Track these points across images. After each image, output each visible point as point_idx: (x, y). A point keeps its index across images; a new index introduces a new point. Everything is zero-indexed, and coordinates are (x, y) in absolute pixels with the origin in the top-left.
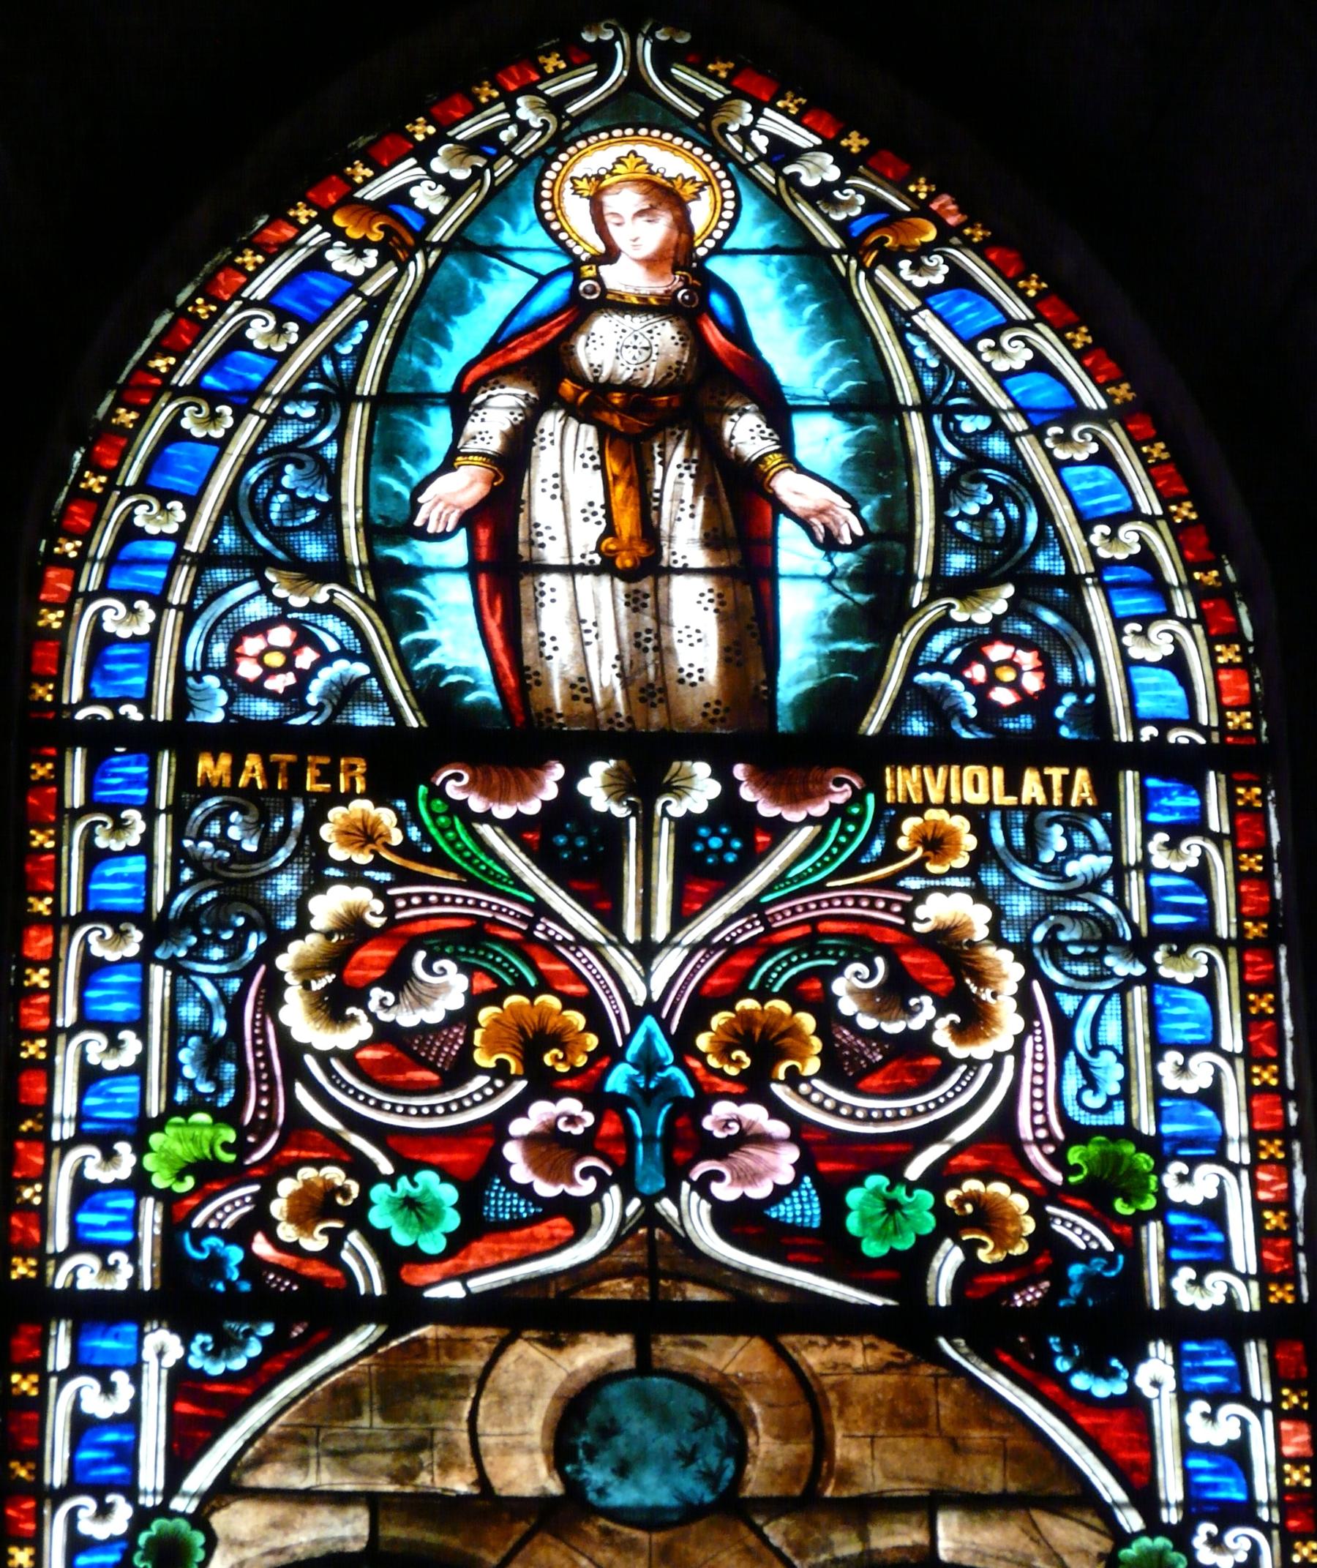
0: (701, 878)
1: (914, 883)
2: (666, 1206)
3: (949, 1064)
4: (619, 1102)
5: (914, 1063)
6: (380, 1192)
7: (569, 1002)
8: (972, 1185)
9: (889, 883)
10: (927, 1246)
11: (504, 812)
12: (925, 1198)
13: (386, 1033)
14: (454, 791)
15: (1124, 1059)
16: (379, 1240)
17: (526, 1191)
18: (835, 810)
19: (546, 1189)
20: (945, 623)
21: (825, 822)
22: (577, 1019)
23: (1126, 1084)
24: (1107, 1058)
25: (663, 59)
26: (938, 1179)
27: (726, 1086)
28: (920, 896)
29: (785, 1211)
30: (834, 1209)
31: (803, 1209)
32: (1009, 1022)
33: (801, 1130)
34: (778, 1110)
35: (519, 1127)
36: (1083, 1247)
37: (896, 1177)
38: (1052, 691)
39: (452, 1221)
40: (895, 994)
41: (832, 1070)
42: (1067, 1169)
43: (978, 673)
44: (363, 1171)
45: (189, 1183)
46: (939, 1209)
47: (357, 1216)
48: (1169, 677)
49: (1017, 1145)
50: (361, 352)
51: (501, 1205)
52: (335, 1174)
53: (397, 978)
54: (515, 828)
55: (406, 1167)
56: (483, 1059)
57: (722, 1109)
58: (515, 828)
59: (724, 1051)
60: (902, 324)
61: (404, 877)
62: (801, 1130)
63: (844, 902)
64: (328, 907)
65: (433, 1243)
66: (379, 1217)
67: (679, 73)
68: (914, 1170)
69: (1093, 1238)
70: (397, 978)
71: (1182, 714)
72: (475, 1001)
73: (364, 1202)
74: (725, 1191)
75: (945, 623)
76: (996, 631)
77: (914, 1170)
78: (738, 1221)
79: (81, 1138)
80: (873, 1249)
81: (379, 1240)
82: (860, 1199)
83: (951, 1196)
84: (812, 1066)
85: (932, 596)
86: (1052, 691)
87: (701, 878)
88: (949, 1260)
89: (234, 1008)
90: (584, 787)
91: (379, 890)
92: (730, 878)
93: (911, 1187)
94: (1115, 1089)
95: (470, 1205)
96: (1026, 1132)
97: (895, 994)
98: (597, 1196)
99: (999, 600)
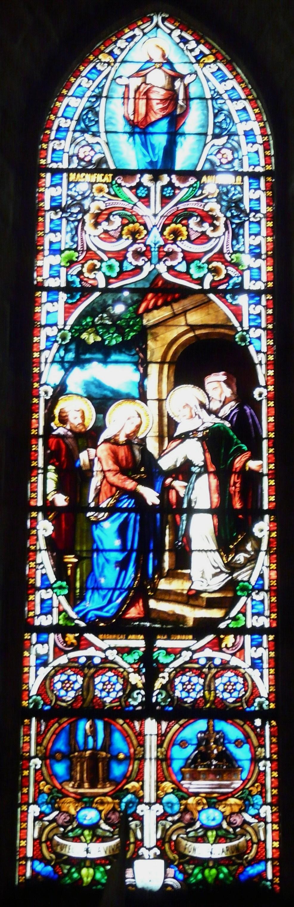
0: (165, 200)
1: (206, 201)
2: (158, 266)
4: (149, 245)
5: (204, 238)
7: (141, 224)
9: (201, 201)
10: (205, 275)
11: (128, 185)
12: (206, 265)
13: (106, 232)
14: (119, 181)
18: (191, 186)
20: (213, 145)
21: (189, 187)
22: (142, 228)
25: (164, 20)
27: (169, 242)
28: (206, 203)
29: (178, 268)
30: (188, 268)
31: (182, 268)
32: (222, 229)
33: (183, 251)
34: (178, 246)
38: (234, 159)
40: (200, 223)
41: (189, 239)
43: (219, 156)
44: (101, 261)
45: (68, 264)
48: (256, 155)
49: (224, 254)
50: (103, 86)
51: (127, 266)
52: (95, 262)
53: (108, 220)
54: (131, 188)
55: (110, 258)
57: (168, 246)
58: (131, 188)
59: (169, 234)
60: (208, 81)
61: (109, 200)
62: (183, 251)
63: (192, 204)
64: (94, 209)
65: (114, 275)
66: (104, 269)
67: (166, 23)
68: (204, 259)
70: (108, 220)
71: (257, 163)
72: (123, 225)
74: (169, 263)
75: (213, 145)
76: (224, 146)
77: (204, 259)
78: (171, 269)
80: (195, 276)
82: (193, 266)
84: (185, 238)
85: (213, 139)
86: (234, 159)
87: (165, 200)
89: (76, 228)
90: (143, 180)
91: (104, 202)
92: (171, 198)
95: (121, 266)
96: (225, 251)
97: (200, 223)
99: (224, 140)
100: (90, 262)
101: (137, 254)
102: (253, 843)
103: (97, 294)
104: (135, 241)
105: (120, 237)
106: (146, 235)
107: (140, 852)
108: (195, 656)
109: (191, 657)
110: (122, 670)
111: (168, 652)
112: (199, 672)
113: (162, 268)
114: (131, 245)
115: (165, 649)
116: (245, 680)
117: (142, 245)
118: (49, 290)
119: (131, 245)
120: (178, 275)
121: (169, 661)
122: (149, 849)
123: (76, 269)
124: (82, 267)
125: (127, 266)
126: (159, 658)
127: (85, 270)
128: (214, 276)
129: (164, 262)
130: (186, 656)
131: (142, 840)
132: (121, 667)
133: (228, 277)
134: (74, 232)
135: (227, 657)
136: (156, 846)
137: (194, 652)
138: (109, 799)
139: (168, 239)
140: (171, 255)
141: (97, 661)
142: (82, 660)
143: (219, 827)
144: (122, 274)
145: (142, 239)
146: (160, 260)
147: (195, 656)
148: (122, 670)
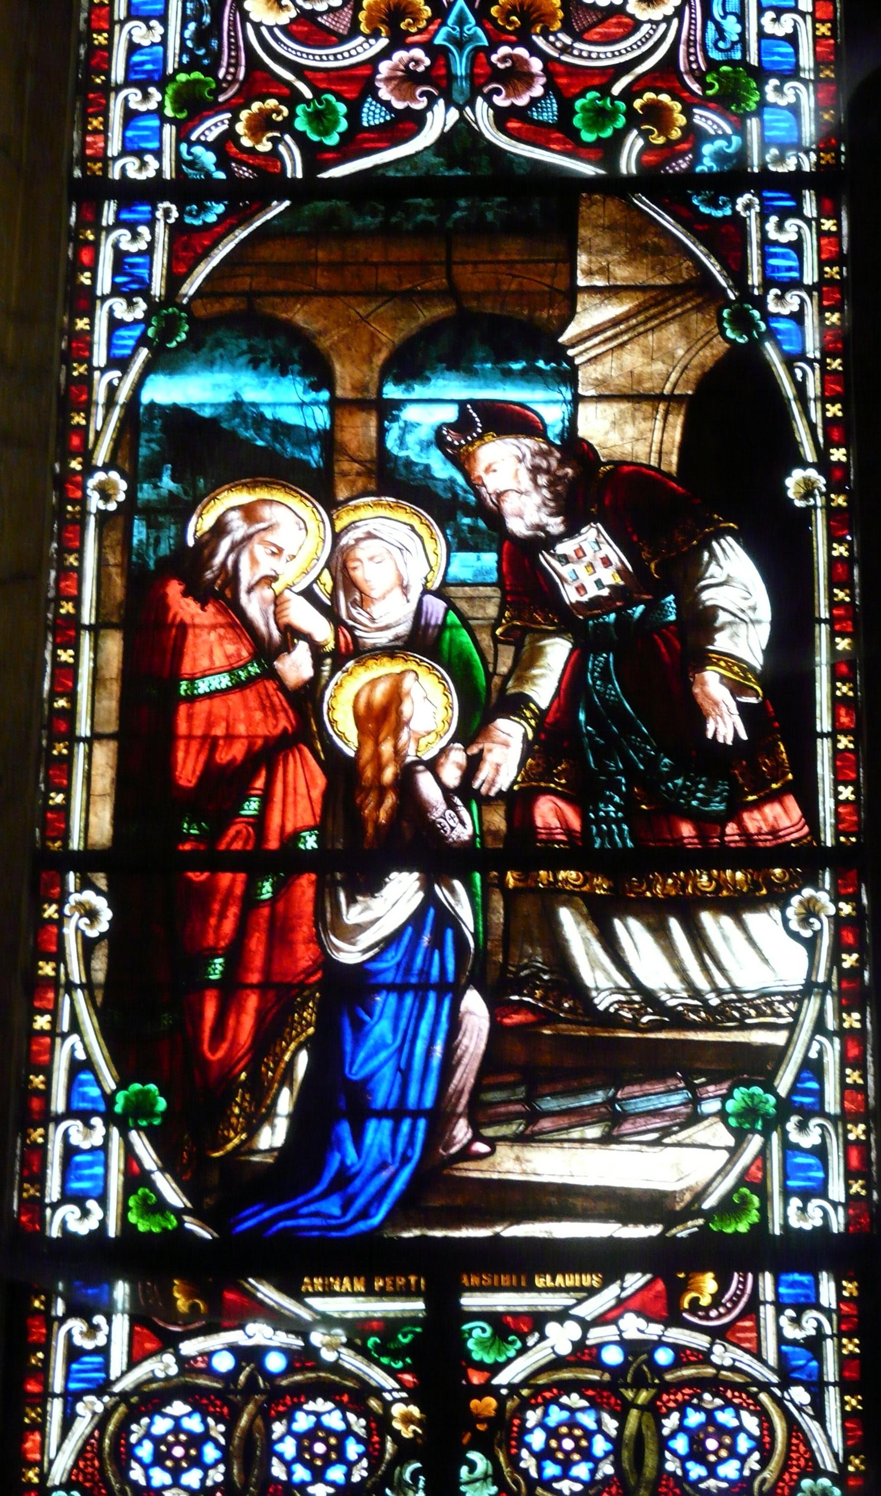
3: (637, 24)
6: (300, 109)
8: (649, 96)
10: (620, 136)
12: (622, 106)
15: (741, 19)
16: (300, 138)
17: (387, 104)
19: (399, 105)
23: (742, 35)
24: (732, 19)
26: (629, 95)
30: (566, 111)
35: (384, 68)
36: (712, 132)
37: (605, 91)
39: (343, 125)
42: (705, 86)
44: (292, 98)
46: (630, 113)
47: (287, 126)
51: (372, 115)
56: (363, 28)
65: (333, 140)
66: (300, 124)
68: (616, 90)
69: (719, 126)
73: (293, 115)
79: (128, 83)
81: (300, 138)
83: (637, 104)
88: (633, 143)
93: (614, 99)
94: (736, 38)
95: (354, 116)
98: (429, 107)
100: (256, 106)
101: (408, 79)
103: (278, 208)
104: (399, 41)
105: (354, 31)
106: (430, 21)
109: (579, 1346)
111: (504, 1327)
112: (607, 1395)
113: (482, 116)
114: (385, 54)
115: (492, 1318)
116: (763, 1415)
117: (418, 53)
118: (131, 194)
119: (385, 54)
120: (537, 134)
121: (502, 1359)
123: (212, 128)
124: (234, 120)
125: (372, 115)
127: (240, 128)
128: (645, 134)
129: (488, 98)
130: (561, 1338)
133: (695, 135)
134: (207, 19)
135: (701, 1341)
137: (586, 1325)
139: (503, 30)
140: (517, 77)
144: (356, 142)
145: (420, 32)
146: (475, 91)
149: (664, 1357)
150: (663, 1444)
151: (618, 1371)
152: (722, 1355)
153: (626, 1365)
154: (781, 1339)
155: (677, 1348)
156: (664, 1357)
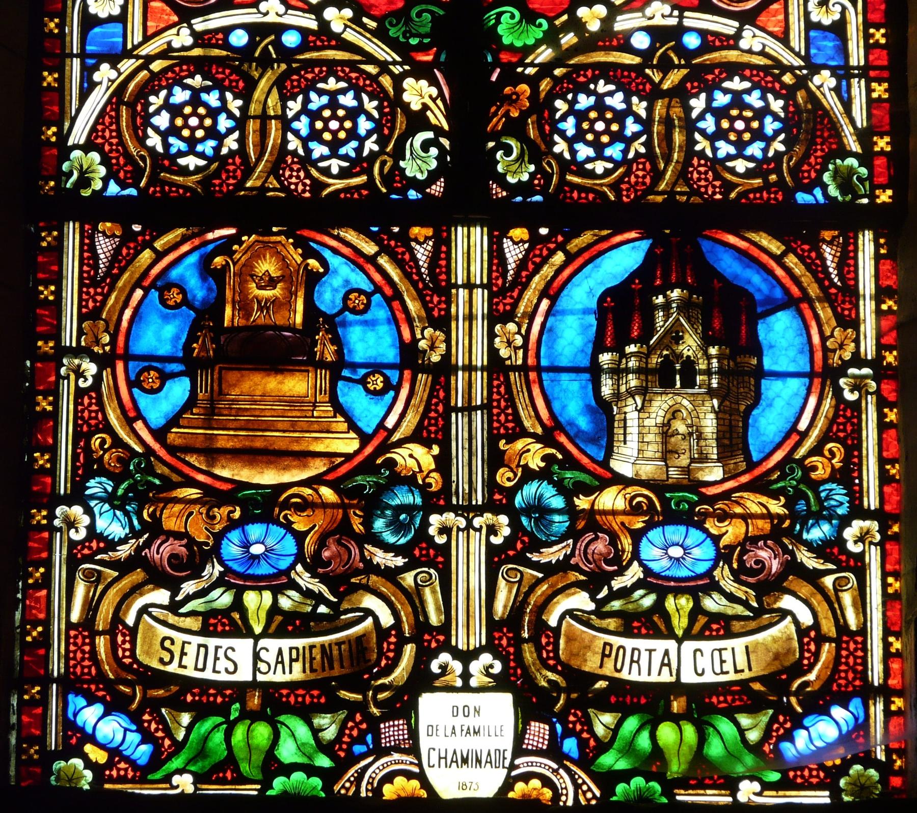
102: (821, 639)
107: (435, 667)
108: (622, 23)
110: (371, 69)
121: (530, 42)
122: (465, 657)
126: (501, 30)
131: (446, 628)
132: (370, 59)
135: (727, 26)
136: (490, 646)
138: (327, 493)
141: (291, 39)
142: (239, 39)
143: (705, 584)
147: (622, 23)
148: (371, 69)
149: (692, 41)
150: (690, 126)
151: (646, 55)
152: (752, 39)
153: (652, 50)
154: (810, 26)
155: (703, 33)
156: (692, 41)
